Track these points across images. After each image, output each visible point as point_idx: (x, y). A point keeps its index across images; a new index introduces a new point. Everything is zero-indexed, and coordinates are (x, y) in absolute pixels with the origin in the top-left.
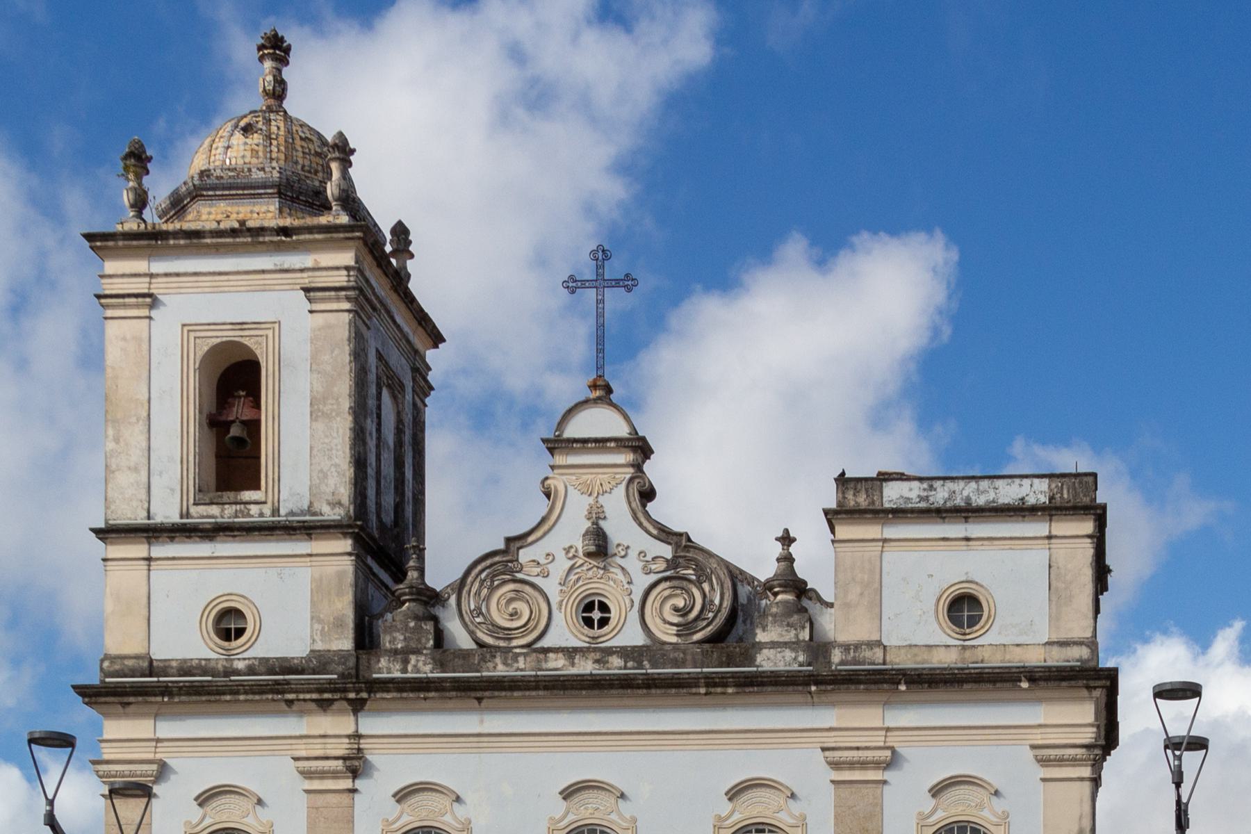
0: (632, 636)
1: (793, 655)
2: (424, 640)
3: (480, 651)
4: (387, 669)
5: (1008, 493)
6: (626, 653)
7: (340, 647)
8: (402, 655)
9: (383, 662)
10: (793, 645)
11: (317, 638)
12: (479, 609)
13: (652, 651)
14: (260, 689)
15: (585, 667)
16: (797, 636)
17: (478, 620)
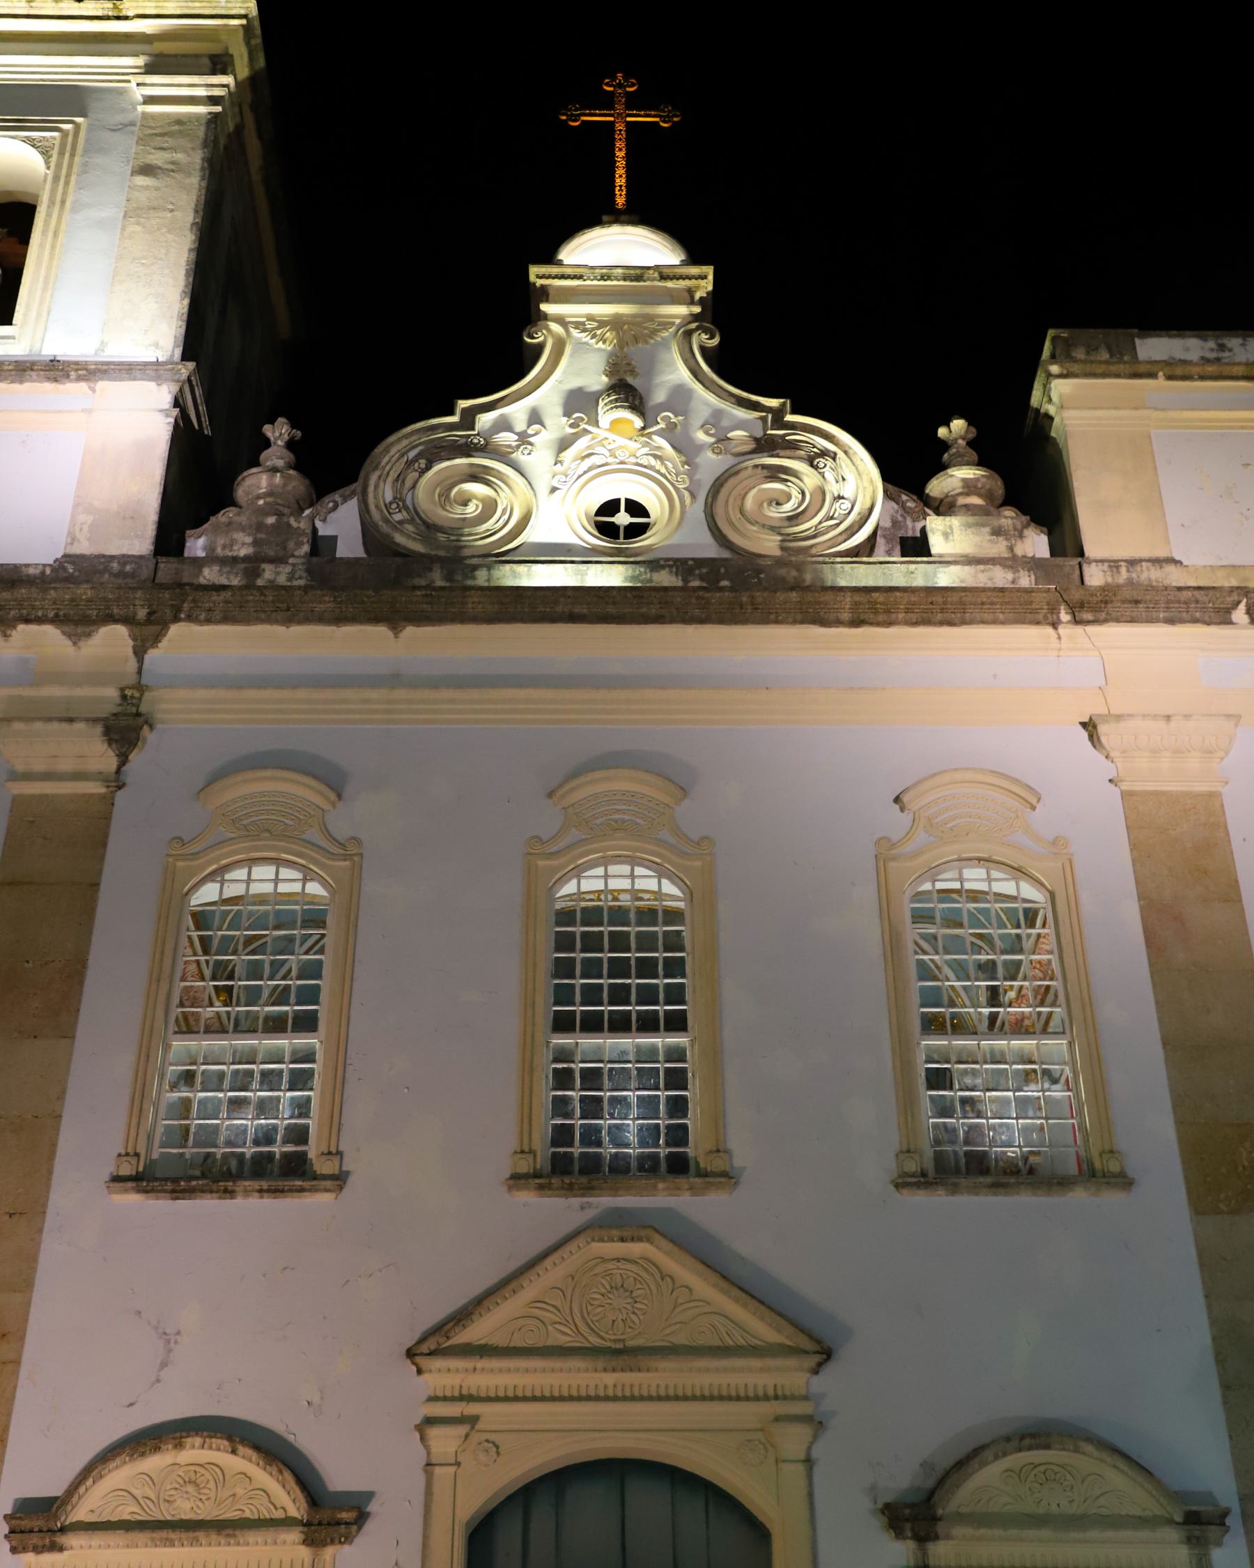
1: (1010, 576)
2: (291, 545)
3: (399, 560)
7: (125, 551)
9: (206, 571)
11: (82, 537)
12: (398, 499)
16: (1011, 549)
17: (398, 517)
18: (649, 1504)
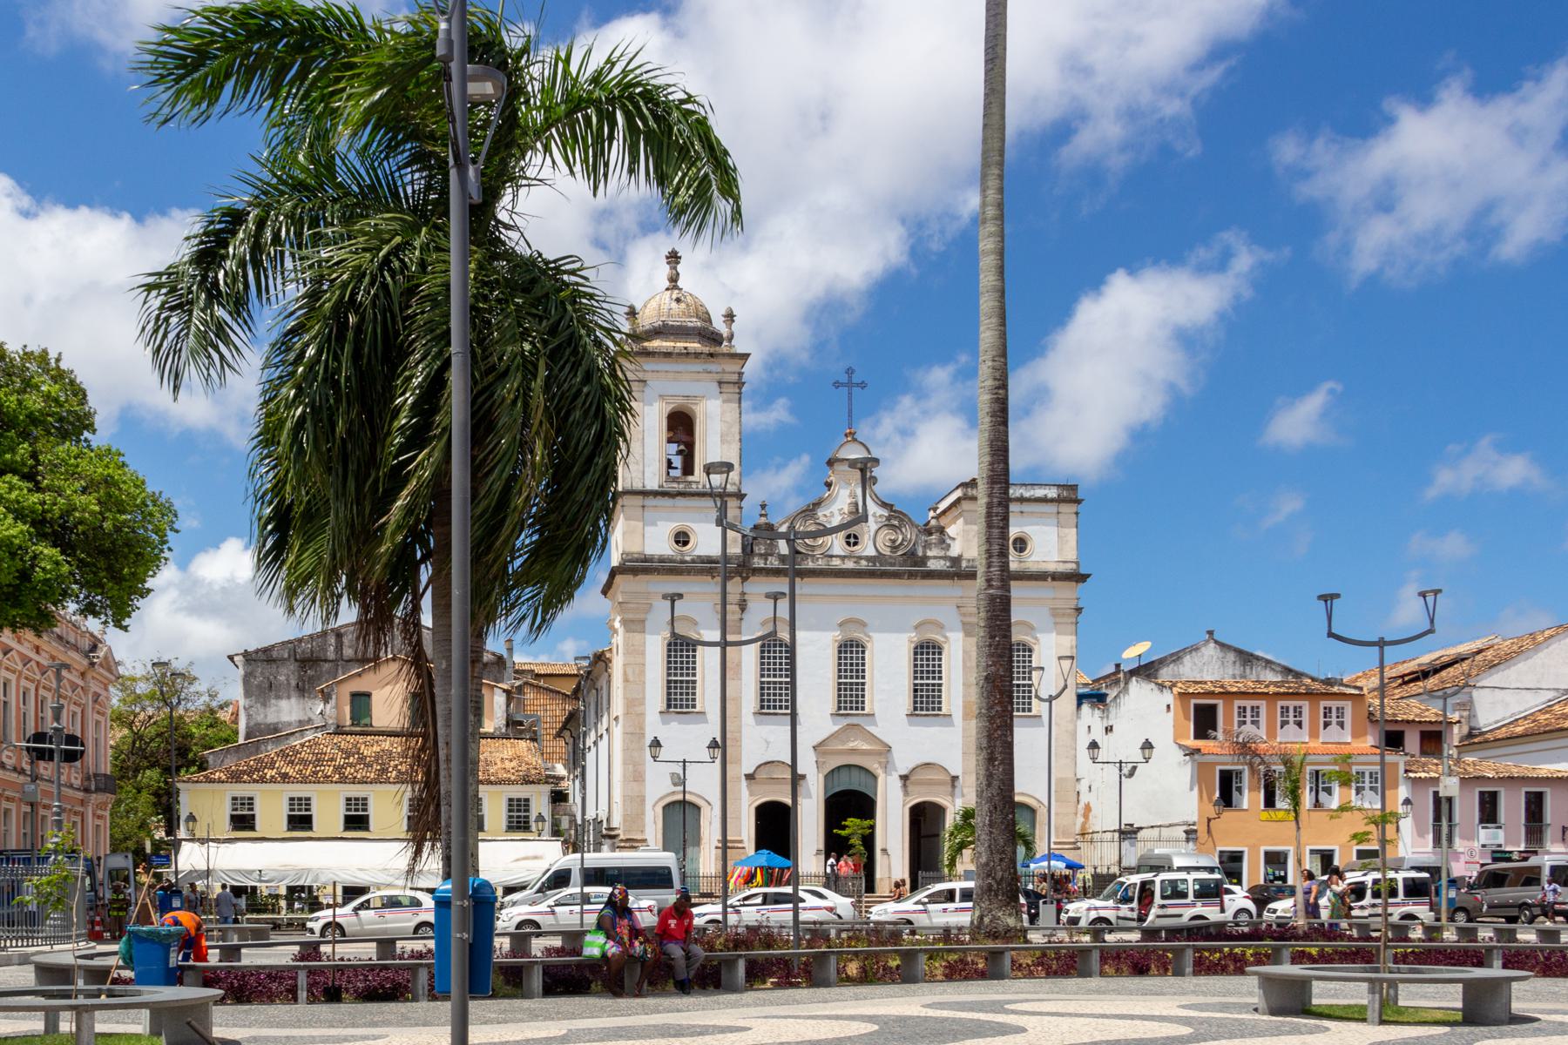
0: (871, 552)
4: (758, 562)
5: (1039, 493)
6: (868, 559)
8: (765, 556)
10: (945, 558)
13: (880, 557)
14: (701, 572)
15: (850, 565)
18: (855, 772)
